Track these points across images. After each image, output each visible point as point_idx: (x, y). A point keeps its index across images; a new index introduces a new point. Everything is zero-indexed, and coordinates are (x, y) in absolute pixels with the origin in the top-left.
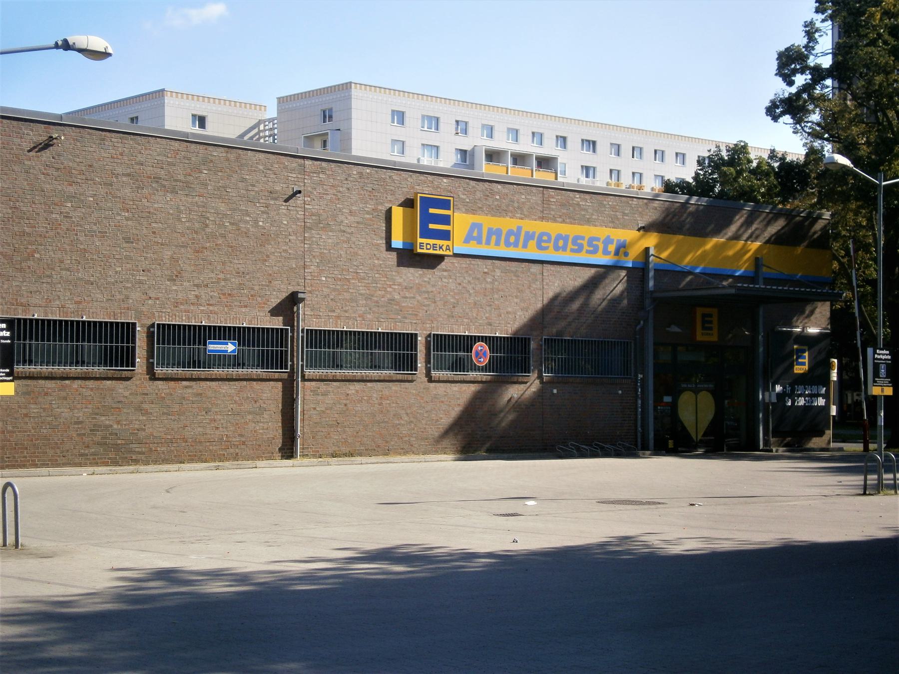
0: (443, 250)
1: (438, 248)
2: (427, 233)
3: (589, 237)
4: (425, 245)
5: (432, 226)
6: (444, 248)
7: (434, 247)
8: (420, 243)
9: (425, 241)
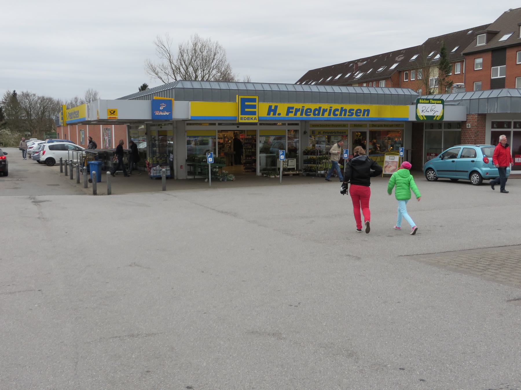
0: (253, 120)
1: (250, 119)
2: (243, 113)
3: (349, 109)
4: (243, 118)
5: (246, 110)
6: (253, 119)
7: (248, 119)
8: (241, 118)
9: (243, 116)
